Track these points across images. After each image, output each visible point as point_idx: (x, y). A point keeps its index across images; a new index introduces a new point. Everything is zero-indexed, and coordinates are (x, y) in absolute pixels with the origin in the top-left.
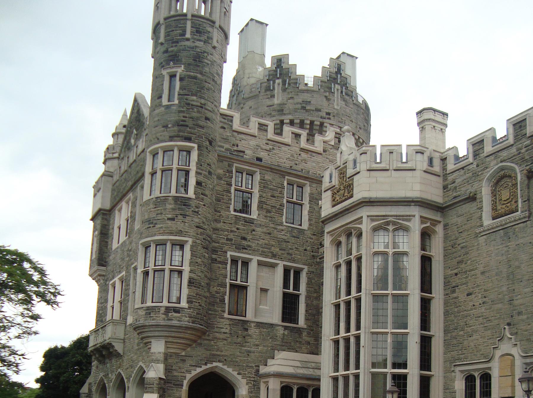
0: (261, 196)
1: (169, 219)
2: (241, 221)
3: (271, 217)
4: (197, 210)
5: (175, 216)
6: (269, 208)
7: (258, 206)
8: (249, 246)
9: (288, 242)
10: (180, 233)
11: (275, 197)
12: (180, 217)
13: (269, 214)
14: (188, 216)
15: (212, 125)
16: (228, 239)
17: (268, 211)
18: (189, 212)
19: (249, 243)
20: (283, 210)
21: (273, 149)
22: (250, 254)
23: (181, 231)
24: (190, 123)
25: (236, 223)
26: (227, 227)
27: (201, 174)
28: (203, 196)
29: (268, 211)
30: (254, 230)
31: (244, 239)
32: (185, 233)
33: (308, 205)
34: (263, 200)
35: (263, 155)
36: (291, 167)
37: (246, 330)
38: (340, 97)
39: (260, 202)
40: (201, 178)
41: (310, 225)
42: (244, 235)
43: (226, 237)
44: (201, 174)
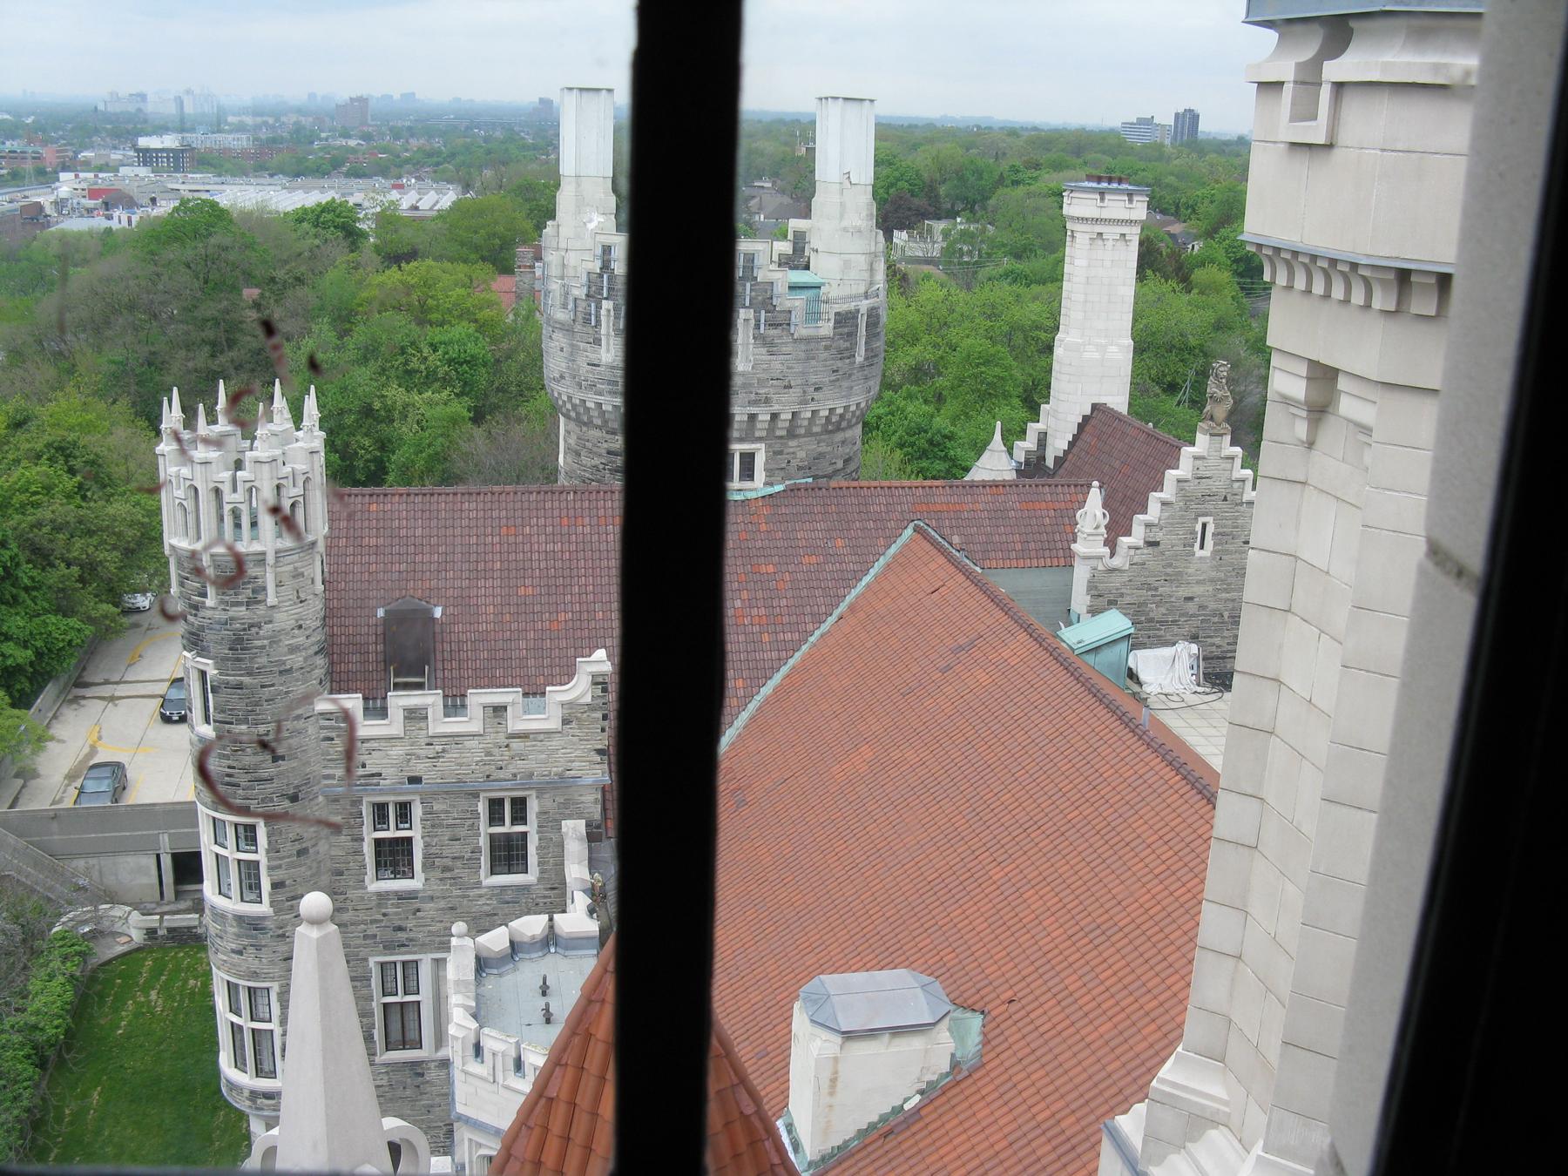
0: (427, 845)
1: (233, 951)
2: (390, 899)
3: (454, 879)
4: (281, 932)
5: (241, 947)
6: (449, 862)
7: (424, 865)
8: (411, 940)
9: (495, 915)
10: (254, 975)
11: (459, 839)
12: (251, 950)
13: (448, 875)
14: (264, 946)
15: (294, 764)
16: (366, 937)
17: (446, 869)
18: (265, 940)
19: (412, 935)
20: (479, 859)
21: (444, 751)
22: (415, 953)
23: (255, 972)
24: (242, 779)
25: (379, 905)
26: (362, 916)
27: (280, 867)
28: (289, 903)
29: (446, 869)
30: (419, 910)
31: (400, 929)
32: (263, 976)
33: (536, 837)
34: (433, 850)
35: (419, 768)
36: (488, 776)
37: (422, 1075)
38: (754, 338)
39: (426, 856)
40: (280, 875)
41: (542, 872)
42: (398, 923)
43: (362, 935)
44: (280, 867)
